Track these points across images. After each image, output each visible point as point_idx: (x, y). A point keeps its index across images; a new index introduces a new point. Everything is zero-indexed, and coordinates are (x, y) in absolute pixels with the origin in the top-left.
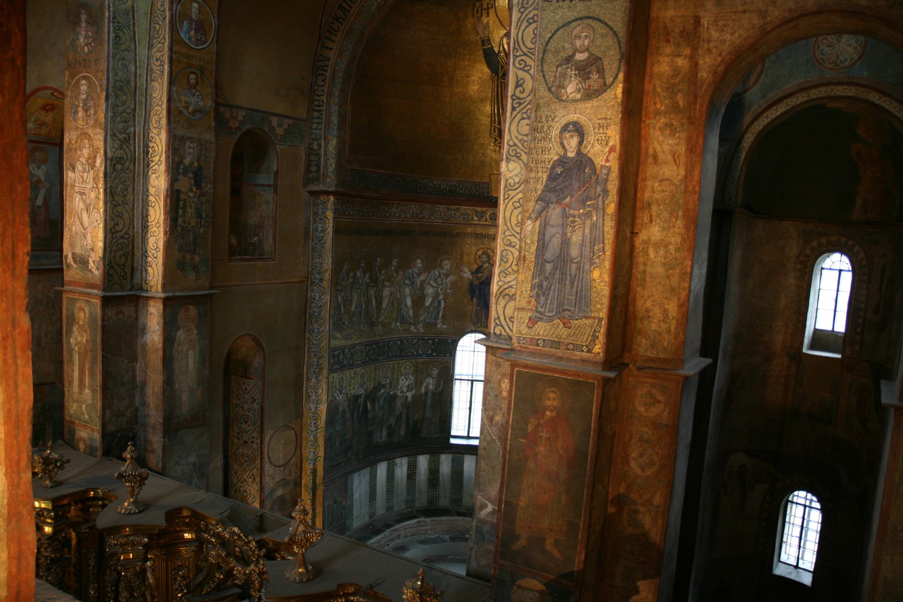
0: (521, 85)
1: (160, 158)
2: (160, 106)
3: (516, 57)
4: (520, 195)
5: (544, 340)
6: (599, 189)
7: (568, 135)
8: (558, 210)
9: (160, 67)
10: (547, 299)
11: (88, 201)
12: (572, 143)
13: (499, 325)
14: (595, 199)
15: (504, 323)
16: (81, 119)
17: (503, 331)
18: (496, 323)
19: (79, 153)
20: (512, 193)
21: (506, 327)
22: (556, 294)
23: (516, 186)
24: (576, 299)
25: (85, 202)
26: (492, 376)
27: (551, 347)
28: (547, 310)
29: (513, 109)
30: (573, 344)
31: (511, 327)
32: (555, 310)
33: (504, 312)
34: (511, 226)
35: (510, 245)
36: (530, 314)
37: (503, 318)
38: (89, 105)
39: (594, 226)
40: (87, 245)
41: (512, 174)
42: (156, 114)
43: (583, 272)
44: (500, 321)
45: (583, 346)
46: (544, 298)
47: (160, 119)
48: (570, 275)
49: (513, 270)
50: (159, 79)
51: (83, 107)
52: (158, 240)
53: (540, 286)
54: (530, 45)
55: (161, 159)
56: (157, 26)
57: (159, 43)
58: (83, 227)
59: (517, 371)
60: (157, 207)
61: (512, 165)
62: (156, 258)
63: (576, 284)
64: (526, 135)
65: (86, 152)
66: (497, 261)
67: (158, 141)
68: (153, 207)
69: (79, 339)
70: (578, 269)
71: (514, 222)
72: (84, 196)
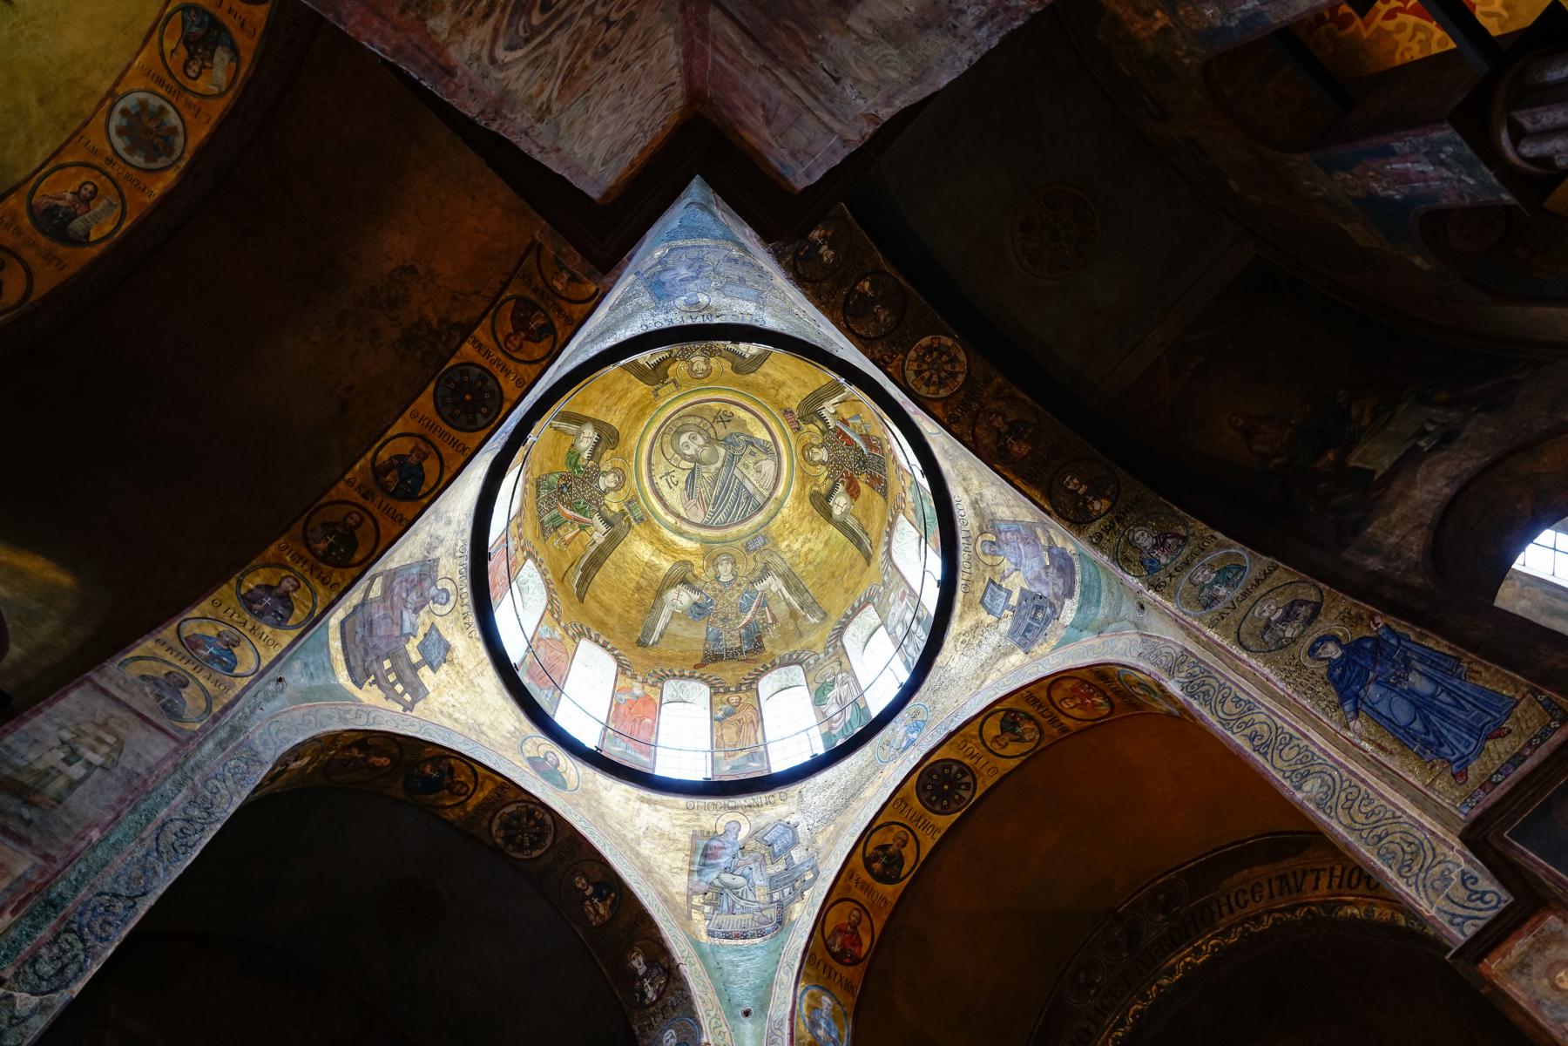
0: (1256, 736)
3: (1231, 729)
4: (1343, 795)
5: (1498, 772)
6: (1393, 642)
7: (1320, 651)
8: (1372, 688)
10: (1449, 744)
12: (1333, 651)
13: (1464, 922)
14: (1398, 648)
15: (1466, 912)
17: (1477, 921)
18: (1458, 924)
21: (1476, 913)
22: (1454, 729)
23: (1330, 793)
24: (1479, 708)
26: (1534, 992)
27: (1516, 767)
28: (1463, 750)
29: (1264, 755)
30: (1535, 737)
31: (1483, 906)
32: (1471, 740)
33: (1453, 902)
34: (1363, 824)
35: (1380, 839)
36: (1448, 775)
37: (1459, 908)
39: (1421, 660)
41: (1315, 790)
43: (1459, 689)
44: (1461, 916)
45: (1549, 725)
46: (1446, 746)
48: (1448, 704)
49: (1412, 853)
53: (1426, 745)
54: (1238, 710)
59: (1508, 835)
61: (1307, 787)
63: (1463, 702)
64: (1298, 754)
66: (1382, 867)
70: (1449, 693)
71: (1360, 818)
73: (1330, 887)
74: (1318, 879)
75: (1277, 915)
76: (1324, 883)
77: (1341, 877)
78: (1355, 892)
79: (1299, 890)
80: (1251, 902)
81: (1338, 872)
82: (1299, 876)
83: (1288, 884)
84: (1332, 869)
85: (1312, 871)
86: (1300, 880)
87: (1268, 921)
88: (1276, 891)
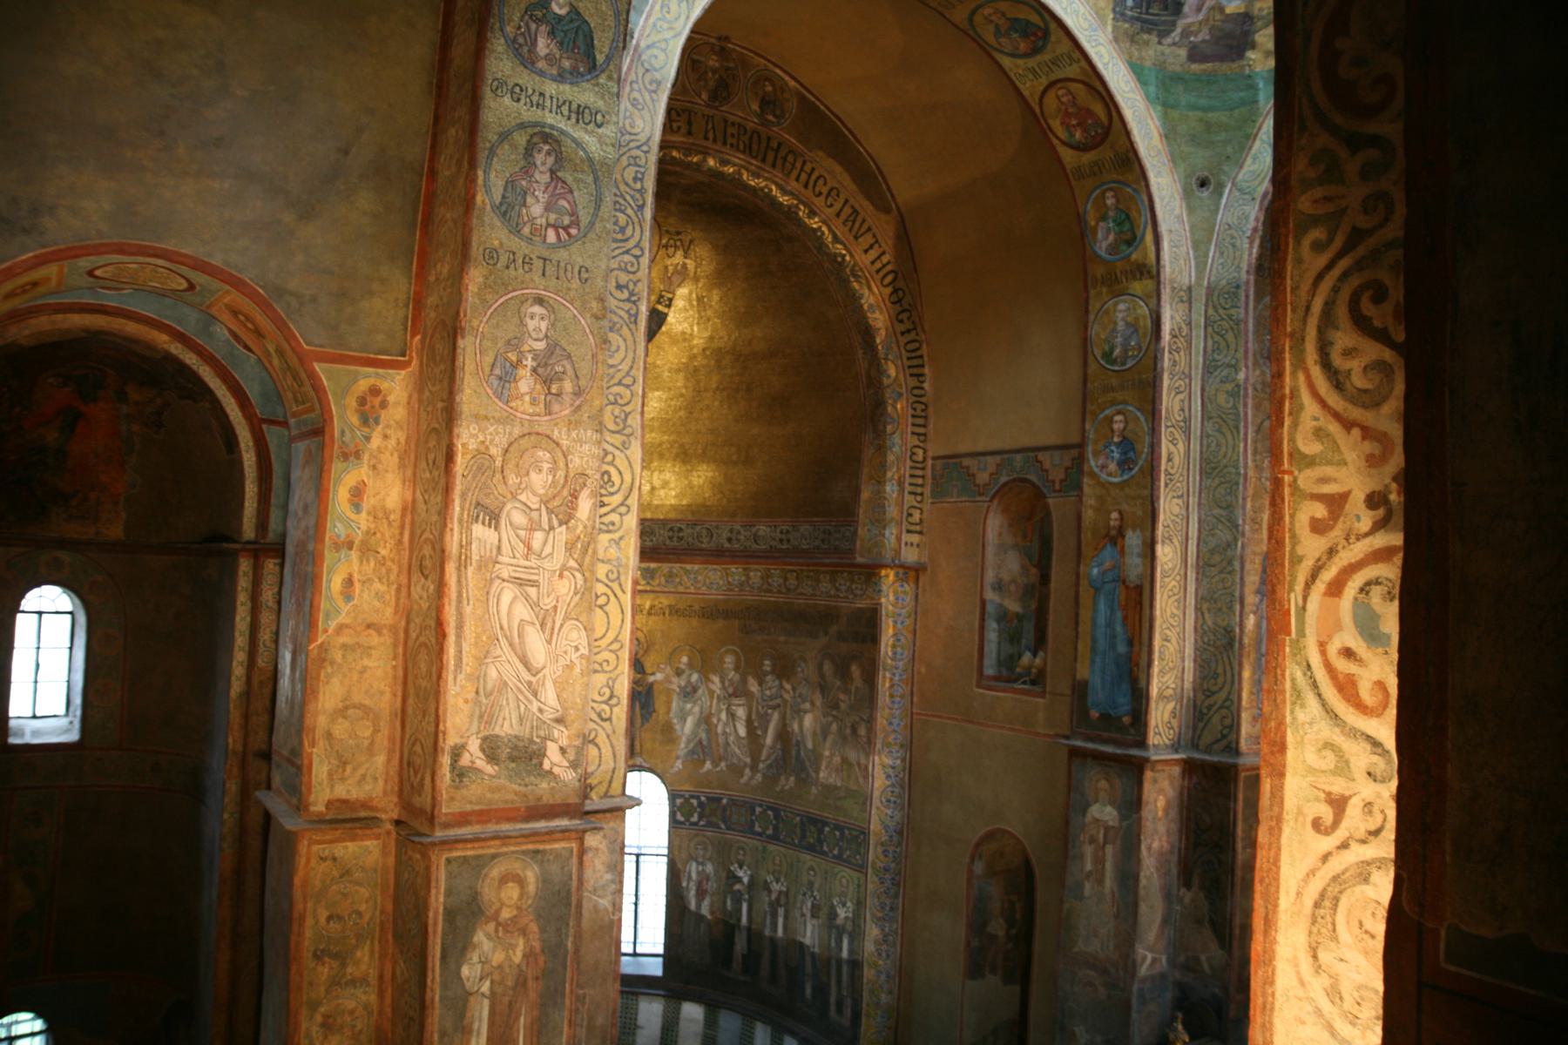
1: (626, 498)
2: (627, 386)
9: (627, 306)
11: (548, 602)
16: (527, 398)
19: (512, 479)
20: (1167, 580)
25: (534, 605)
38: (559, 369)
40: (540, 710)
42: (615, 403)
47: (627, 415)
50: (625, 327)
51: (534, 370)
52: (614, 680)
55: (628, 502)
56: (622, 219)
57: (627, 252)
58: (526, 664)
60: (613, 608)
62: (609, 719)
65: (540, 481)
67: (621, 462)
68: (601, 607)
69: (498, 957)
72: (532, 591)
73: (873, 263)
74: (871, 247)
75: (824, 229)
76: (873, 254)
77: (884, 266)
78: (882, 289)
79: (856, 238)
80: (822, 198)
81: (885, 259)
82: (865, 227)
83: (854, 221)
84: (884, 253)
85: (874, 236)
86: (863, 230)
87: (814, 223)
88: (844, 216)
